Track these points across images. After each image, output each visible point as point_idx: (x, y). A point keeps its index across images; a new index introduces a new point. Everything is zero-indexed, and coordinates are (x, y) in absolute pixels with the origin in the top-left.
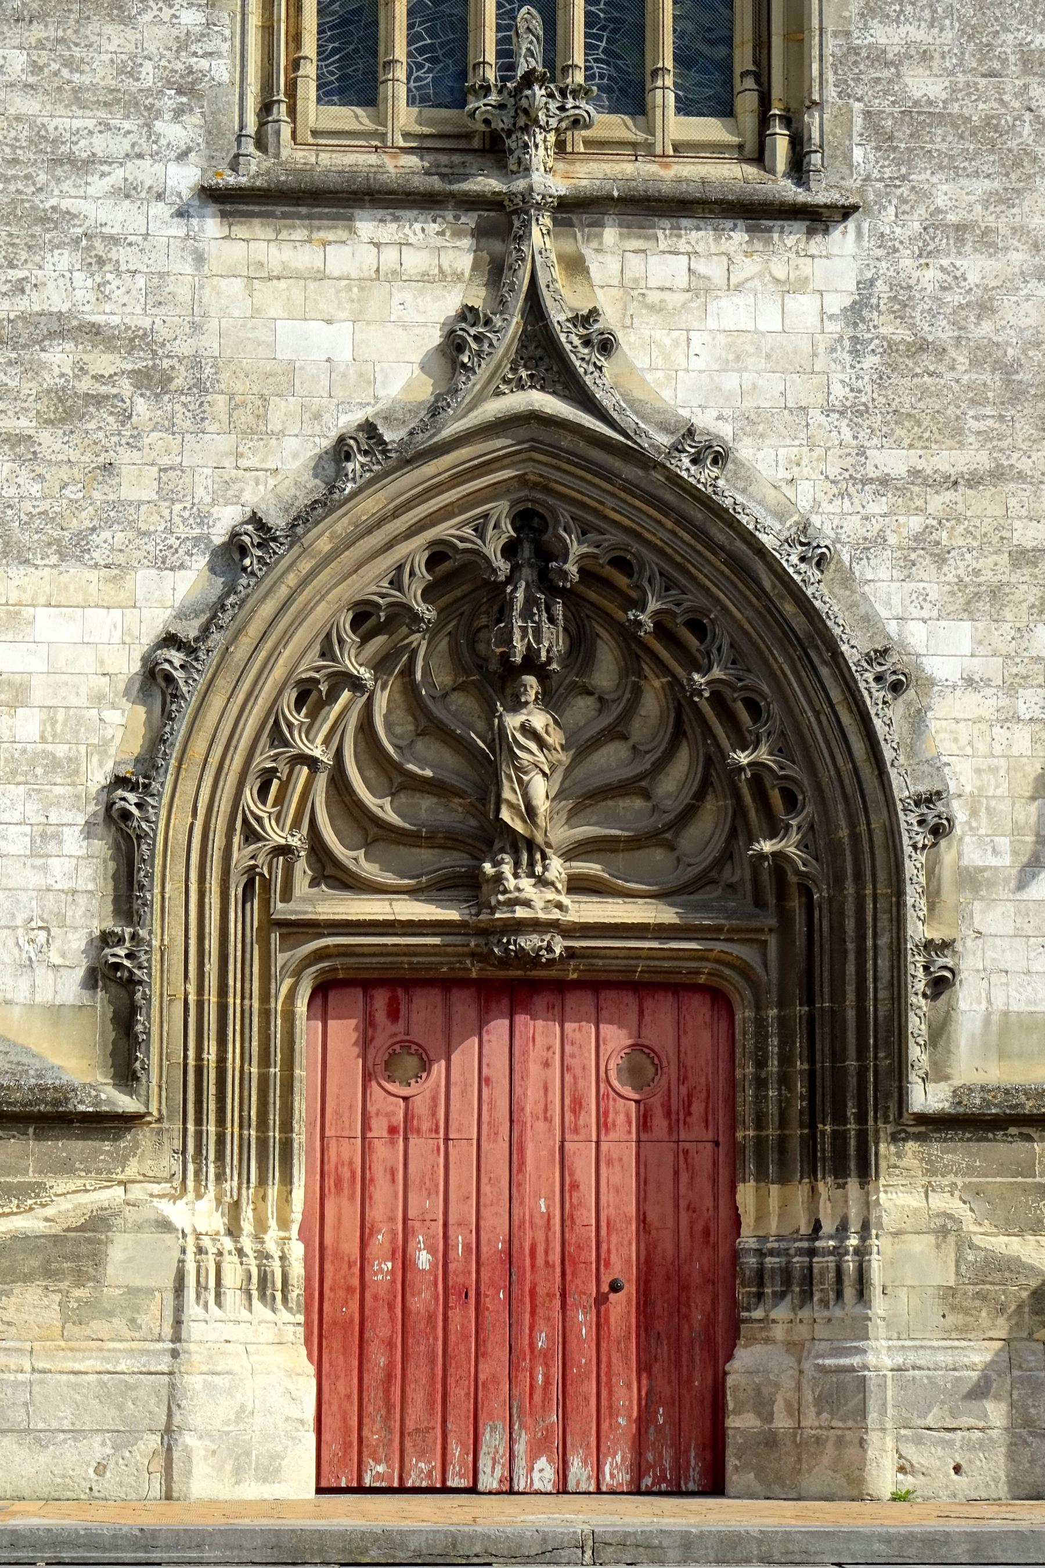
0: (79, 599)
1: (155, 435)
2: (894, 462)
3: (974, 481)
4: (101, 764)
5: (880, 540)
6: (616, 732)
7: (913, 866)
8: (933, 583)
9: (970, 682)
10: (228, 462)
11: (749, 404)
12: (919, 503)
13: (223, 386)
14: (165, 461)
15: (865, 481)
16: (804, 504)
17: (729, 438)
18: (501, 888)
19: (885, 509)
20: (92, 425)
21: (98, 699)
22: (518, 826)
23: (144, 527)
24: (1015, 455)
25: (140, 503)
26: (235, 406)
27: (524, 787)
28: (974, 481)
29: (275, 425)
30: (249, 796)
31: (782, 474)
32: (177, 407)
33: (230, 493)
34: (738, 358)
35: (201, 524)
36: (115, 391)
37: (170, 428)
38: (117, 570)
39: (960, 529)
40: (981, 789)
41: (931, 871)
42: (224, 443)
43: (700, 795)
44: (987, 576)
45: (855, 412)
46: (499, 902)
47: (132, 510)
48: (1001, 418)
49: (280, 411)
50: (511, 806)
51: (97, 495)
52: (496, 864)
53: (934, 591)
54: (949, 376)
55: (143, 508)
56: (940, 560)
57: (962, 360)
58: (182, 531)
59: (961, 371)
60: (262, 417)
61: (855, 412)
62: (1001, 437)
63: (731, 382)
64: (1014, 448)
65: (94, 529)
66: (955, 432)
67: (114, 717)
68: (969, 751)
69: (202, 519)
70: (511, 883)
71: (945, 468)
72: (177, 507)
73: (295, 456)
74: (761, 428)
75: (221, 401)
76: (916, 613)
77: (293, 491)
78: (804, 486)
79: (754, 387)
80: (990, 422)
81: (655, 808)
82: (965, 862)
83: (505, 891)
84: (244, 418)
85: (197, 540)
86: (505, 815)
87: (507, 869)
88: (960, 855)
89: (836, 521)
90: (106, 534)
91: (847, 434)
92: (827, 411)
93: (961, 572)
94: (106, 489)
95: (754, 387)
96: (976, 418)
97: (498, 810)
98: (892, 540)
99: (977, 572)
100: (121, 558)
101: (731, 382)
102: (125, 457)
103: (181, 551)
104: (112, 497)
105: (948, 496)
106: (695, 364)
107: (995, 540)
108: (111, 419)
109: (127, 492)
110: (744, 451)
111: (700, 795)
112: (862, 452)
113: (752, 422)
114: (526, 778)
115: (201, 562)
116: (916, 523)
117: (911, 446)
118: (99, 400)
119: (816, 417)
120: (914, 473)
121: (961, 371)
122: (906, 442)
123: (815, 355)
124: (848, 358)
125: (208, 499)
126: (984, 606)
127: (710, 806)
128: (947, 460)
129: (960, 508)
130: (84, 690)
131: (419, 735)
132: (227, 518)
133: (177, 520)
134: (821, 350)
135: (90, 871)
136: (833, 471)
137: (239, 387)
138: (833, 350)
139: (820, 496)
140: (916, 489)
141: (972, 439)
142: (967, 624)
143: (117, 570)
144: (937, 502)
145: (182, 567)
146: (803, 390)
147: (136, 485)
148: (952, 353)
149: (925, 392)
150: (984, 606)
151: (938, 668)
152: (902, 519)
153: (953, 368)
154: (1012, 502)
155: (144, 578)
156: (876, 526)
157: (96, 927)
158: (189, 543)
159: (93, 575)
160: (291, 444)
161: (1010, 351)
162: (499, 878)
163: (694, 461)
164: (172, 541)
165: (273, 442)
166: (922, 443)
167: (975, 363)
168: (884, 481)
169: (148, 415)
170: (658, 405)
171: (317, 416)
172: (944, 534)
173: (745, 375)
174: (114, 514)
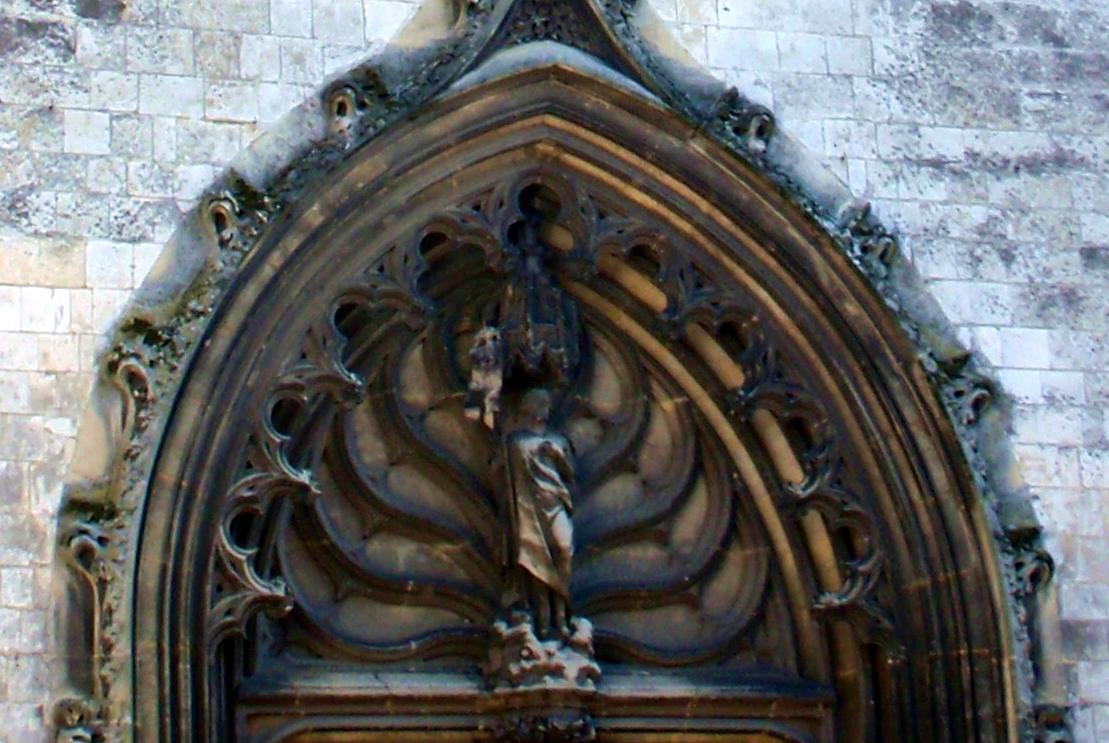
0: (17, 275)
1: (105, 75)
2: (950, 141)
3: (1032, 165)
4: (48, 488)
5: (940, 231)
6: (626, 463)
7: (1012, 620)
8: (1003, 285)
9: (1051, 399)
10: (195, 112)
11: (788, 68)
12: (980, 190)
13: (186, 18)
14: (118, 107)
15: (921, 162)
16: (857, 187)
17: (770, 106)
18: (525, 653)
19: (943, 196)
20: (27, 59)
21: (41, 403)
22: (540, 572)
23: (93, 187)
24: (1076, 139)
25: (90, 157)
26: (201, 41)
27: (547, 527)
28: (1032, 165)
29: (248, 68)
30: (222, 535)
31: (830, 151)
32: (131, 41)
33: (198, 151)
34: (773, 16)
35: (164, 186)
36: (54, 18)
37: (123, 66)
38: (62, 241)
39: (1026, 221)
40: (1074, 527)
41: (1031, 624)
42: (189, 87)
43: (726, 544)
44: (1058, 276)
45: (902, 82)
46: (523, 670)
47: (78, 165)
48: (1057, 97)
49: (255, 53)
50: (530, 546)
51: (35, 146)
52: (511, 623)
53: (1006, 294)
54: (999, 46)
55: (93, 164)
56: (1007, 257)
57: (1010, 29)
58: (142, 194)
59: (1009, 44)
60: (234, 58)
61: (902, 82)
62: (1060, 118)
63: (767, 42)
64: (1074, 132)
65: (32, 188)
66: (1010, 109)
67: (62, 427)
68: (1056, 482)
69: (166, 178)
70: (534, 644)
71: (1003, 150)
72: (134, 165)
73: (275, 108)
74: (804, 96)
75: (184, 35)
76: (988, 318)
77: (274, 150)
78: (853, 164)
79: (793, 48)
80: (1046, 101)
81: (671, 558)
82: (1066, 614)
83: (532, 656)
84: (213, 57)
85: (160, 206)
86: (525, 559)
87: (527, 628)
88: (1059, 607)
89: (900, 206)
90: (47, 195)
91: (896, 108)
92: (875, 79)
93: (1031, 271)
94: (48, 138)
95: (793, 48)
96: (1031, 95)
97: (513, 554)
98: (955, 232)
99: (1047, 272)
100: (66, 226)
101: (767, 42)
102: (68, 99)
103: (141, 221)
104: (55, 149)
105: (1010, 183)
106: (724, 19)
107: (1064, 236)
108: (51, 52)
109: (71, 144)
110: (788, 123)
111: (726, 544)
112: (915, 128)
113: (795, 88)
114: (549, 514)
115: (166, 233)
116: (977, 214)
117: (966, 125)
118: (35, 29)
119: (861, 86)
120: (972, 155)
121: (1009, 44)
122: (961, 119)
123: (855, 15)
124: (891, 20)
125: (172, 156)
126: (1058, 311)
127: (735, 556)
128: (1009, 142)
129: (1023, 197)
130: (23, 392)
131: (392, 464)
132: (196, 179)
133: (133, 178)
134: (861, 9)
135: (36, 628)
136: (885, 150)
137: (204, 20)
138: (874, 11)
139: (874, 178)
140: (975, 174)
141: (1029, 119)
142: (1044, 332)
143: (62, 241)
144: (998, 190)
145: (142, 238)
146: (845, 55)
147: (83, 134)
148: (1000, 20)
149: (977, 64)
150: (1058, 311)
151: (1012, 383)
152: (964, 209)
153: (1002, 38)
154: (1078, 192)
155: (97, 252)
156: (937, 213)
157: (48, 701)
158: (151, 211)
159: (34, 245)
160: (270, 93)
161: (1060, 23)
162: (519, 640)
163: (737, 131)
164: (128, 205)
165: (249, 89)
166: (975, 120)
167: (1025, 34)
168: (938, 164)
169: (96, 49)
170: (689, 65)
171: (299, 60)
172: (1010, 228)
173: (782, 35)
174: (60, 168)
